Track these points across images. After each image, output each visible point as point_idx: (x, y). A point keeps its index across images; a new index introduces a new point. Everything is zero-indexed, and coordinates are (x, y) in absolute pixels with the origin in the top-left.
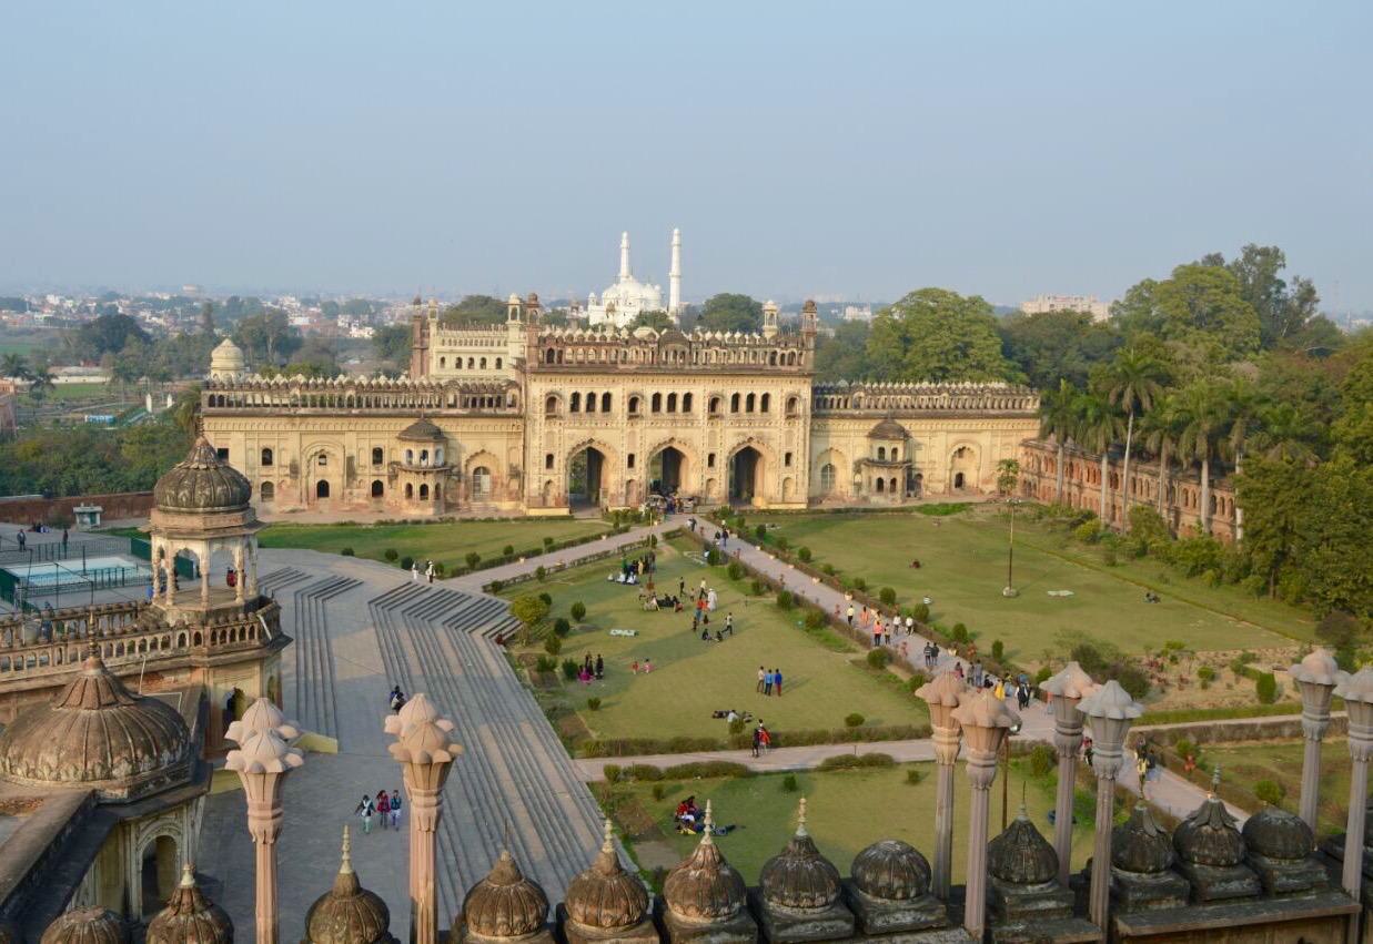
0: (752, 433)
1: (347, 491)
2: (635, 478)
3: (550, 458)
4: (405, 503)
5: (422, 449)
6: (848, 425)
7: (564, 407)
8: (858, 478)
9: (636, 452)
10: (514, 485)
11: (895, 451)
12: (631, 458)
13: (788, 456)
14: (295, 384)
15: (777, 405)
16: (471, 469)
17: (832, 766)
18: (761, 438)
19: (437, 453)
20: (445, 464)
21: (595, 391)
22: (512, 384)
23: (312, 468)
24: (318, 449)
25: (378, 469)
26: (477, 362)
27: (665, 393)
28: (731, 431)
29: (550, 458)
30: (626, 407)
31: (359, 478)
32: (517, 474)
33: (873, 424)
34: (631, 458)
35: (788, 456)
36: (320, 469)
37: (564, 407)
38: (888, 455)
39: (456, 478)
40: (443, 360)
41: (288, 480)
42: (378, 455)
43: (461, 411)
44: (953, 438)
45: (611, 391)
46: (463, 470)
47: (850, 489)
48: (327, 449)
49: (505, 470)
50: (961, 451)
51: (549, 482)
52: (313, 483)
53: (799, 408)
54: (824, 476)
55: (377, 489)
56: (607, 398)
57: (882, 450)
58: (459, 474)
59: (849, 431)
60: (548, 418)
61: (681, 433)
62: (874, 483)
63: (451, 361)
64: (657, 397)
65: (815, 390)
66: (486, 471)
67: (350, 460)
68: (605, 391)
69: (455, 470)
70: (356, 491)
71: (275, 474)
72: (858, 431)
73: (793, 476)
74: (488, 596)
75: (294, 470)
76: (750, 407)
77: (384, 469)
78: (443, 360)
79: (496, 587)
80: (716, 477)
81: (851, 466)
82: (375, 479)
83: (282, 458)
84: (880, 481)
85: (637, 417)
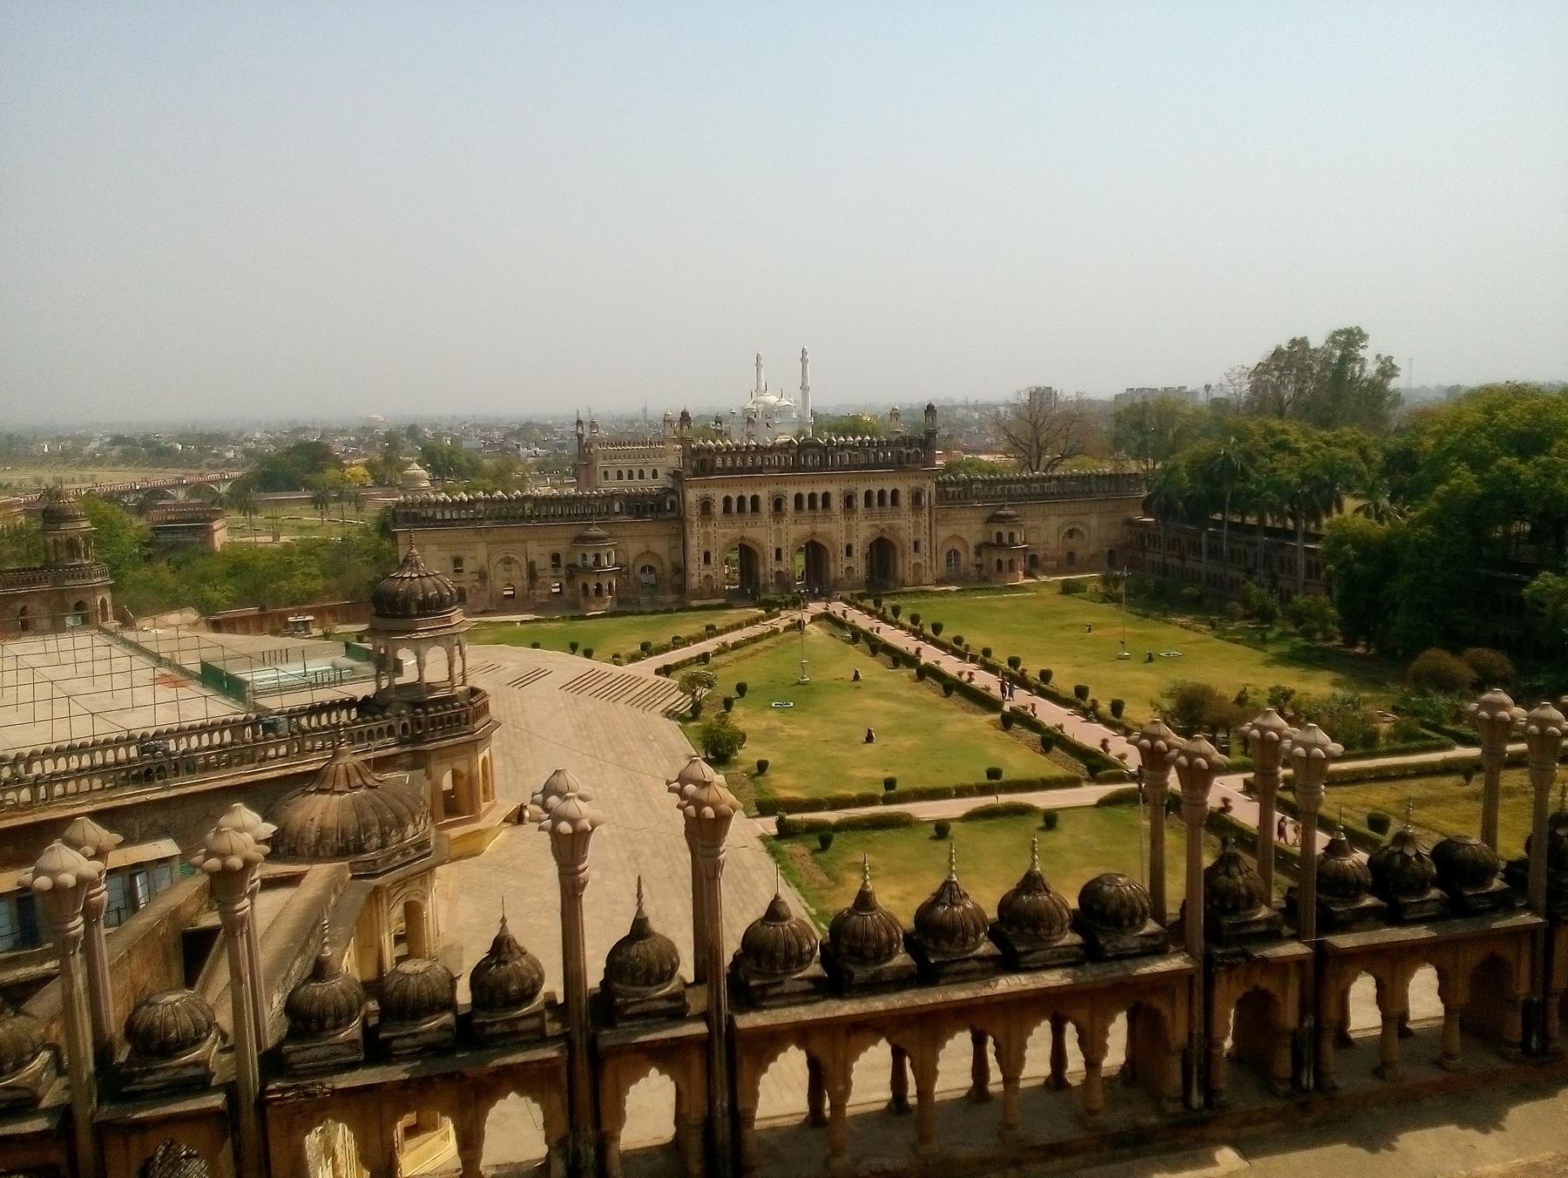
0: (884, 523)
3: (707, 555)
4: (582, 600)
6: (968, 514)
7: (718, 507)
8: (979, 561)
9: (782, 546)
10: (677, 580)
11: (1011, 535)
12: (778, 552)
13: (916, 544)
14: (478, 500)
15: (905, 500)
16: (638, 568)
17: (972, 816)
18: (891, 527)
22: (668, 491)
26: (636, 474)
27: (806, 491)
29: (707, 555)
32: (680, 570)
33: (987, 514)
34: (778, 552)
35: (916, 544)
37: (718, 507)
38: (1006, 539)
40: (606, 473)
42: (556, 558)
44: (1061, 520)
47: (973, 570)
49: (668, 566)
50: (1071, 533)
51: (707, 576)
53: (924, 500)
54: (949, 560)
56: (755, 499)
57: (999, 535)
61: (821, 527)
62: (994, 564)
63: (613, 474)
64: (799, 498)
65: (938, 483)
66: (651, 569)
67: (531, 565)
70: (538, 592)
71: (468, 580)
74: (662, 678)
75: (483, 576)
76: (882, 502)
77: (562, 571)
78: (606, 473)
79: (666, 671)
83: (468, 566)
84: (999, 562)
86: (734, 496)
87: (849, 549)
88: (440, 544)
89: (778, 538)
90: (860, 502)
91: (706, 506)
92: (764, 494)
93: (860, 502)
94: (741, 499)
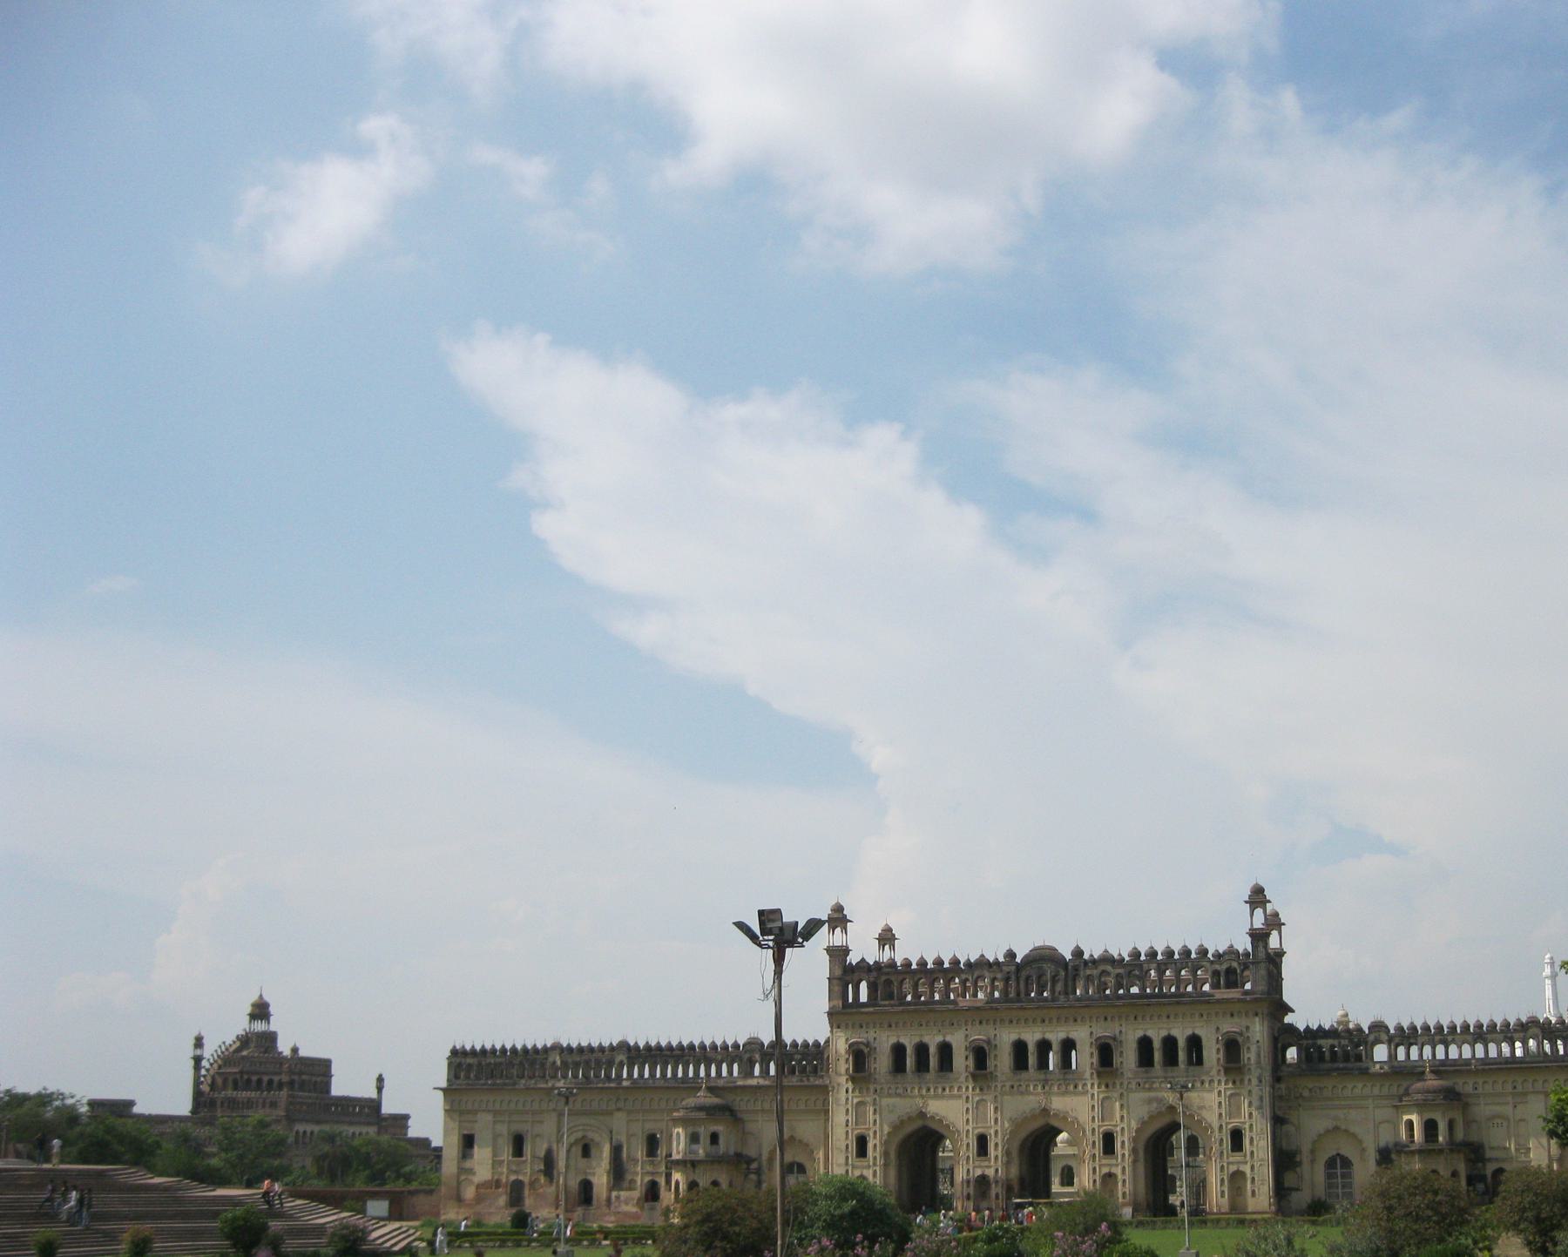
1: (614, 1194)
2: (990, 1172)
3: (862, 1143)
5: (690, 1130)
12: (982, 1141)
15: (1212, 1053)
19: (714, 1138)
20: (739, 1156)
21: (926, 1039)
23: (572, 1163)
24: (580, 1135)
25: (652, 1163)
27: (1031, 1037)
28: (1137, 1097)
29: (862, 1143)
30: (971, 1063)
31: (628, 1177)
34: (982, 1141)
35: (1237, 1137)
36: (582, 1162)
37: (882, 1063)
39: (753, 1177)
41: (542, 1179)
43: (762, 1082)
45: (948, 1038)
46: (764, 1163)
48: (590, 1135)
52: (574, 1184)
53: (1250, 1055)
54: (1329, 1176)
55: (652, 1193)
56: (946, 1050)
57: (1410, 1124)
58: (758, 1172)
59: (1367, 1097)
60: (853, 1079)
61: (1058, 1103)
68: (939, 1039)
69: (754, 1166)
70: (623, 1194)
72: (1381, 1097)
73: (1247, 1169)
75: (549, 1162)
76: (1171, 1059)
80: (1118, 1171)
81: (1372, 1156)
82: (647, 1179)
83: (535, 1149)
85: (985, 1076)
86: (909, 1043)
87: (1109, 1141)
88: (496, 1113)
89: (979, 1117)
90: (1128, 1058)
91: (860, 1057)
92: (958, 1040)
93: (1128, 1058)
94: (922, 1050)
